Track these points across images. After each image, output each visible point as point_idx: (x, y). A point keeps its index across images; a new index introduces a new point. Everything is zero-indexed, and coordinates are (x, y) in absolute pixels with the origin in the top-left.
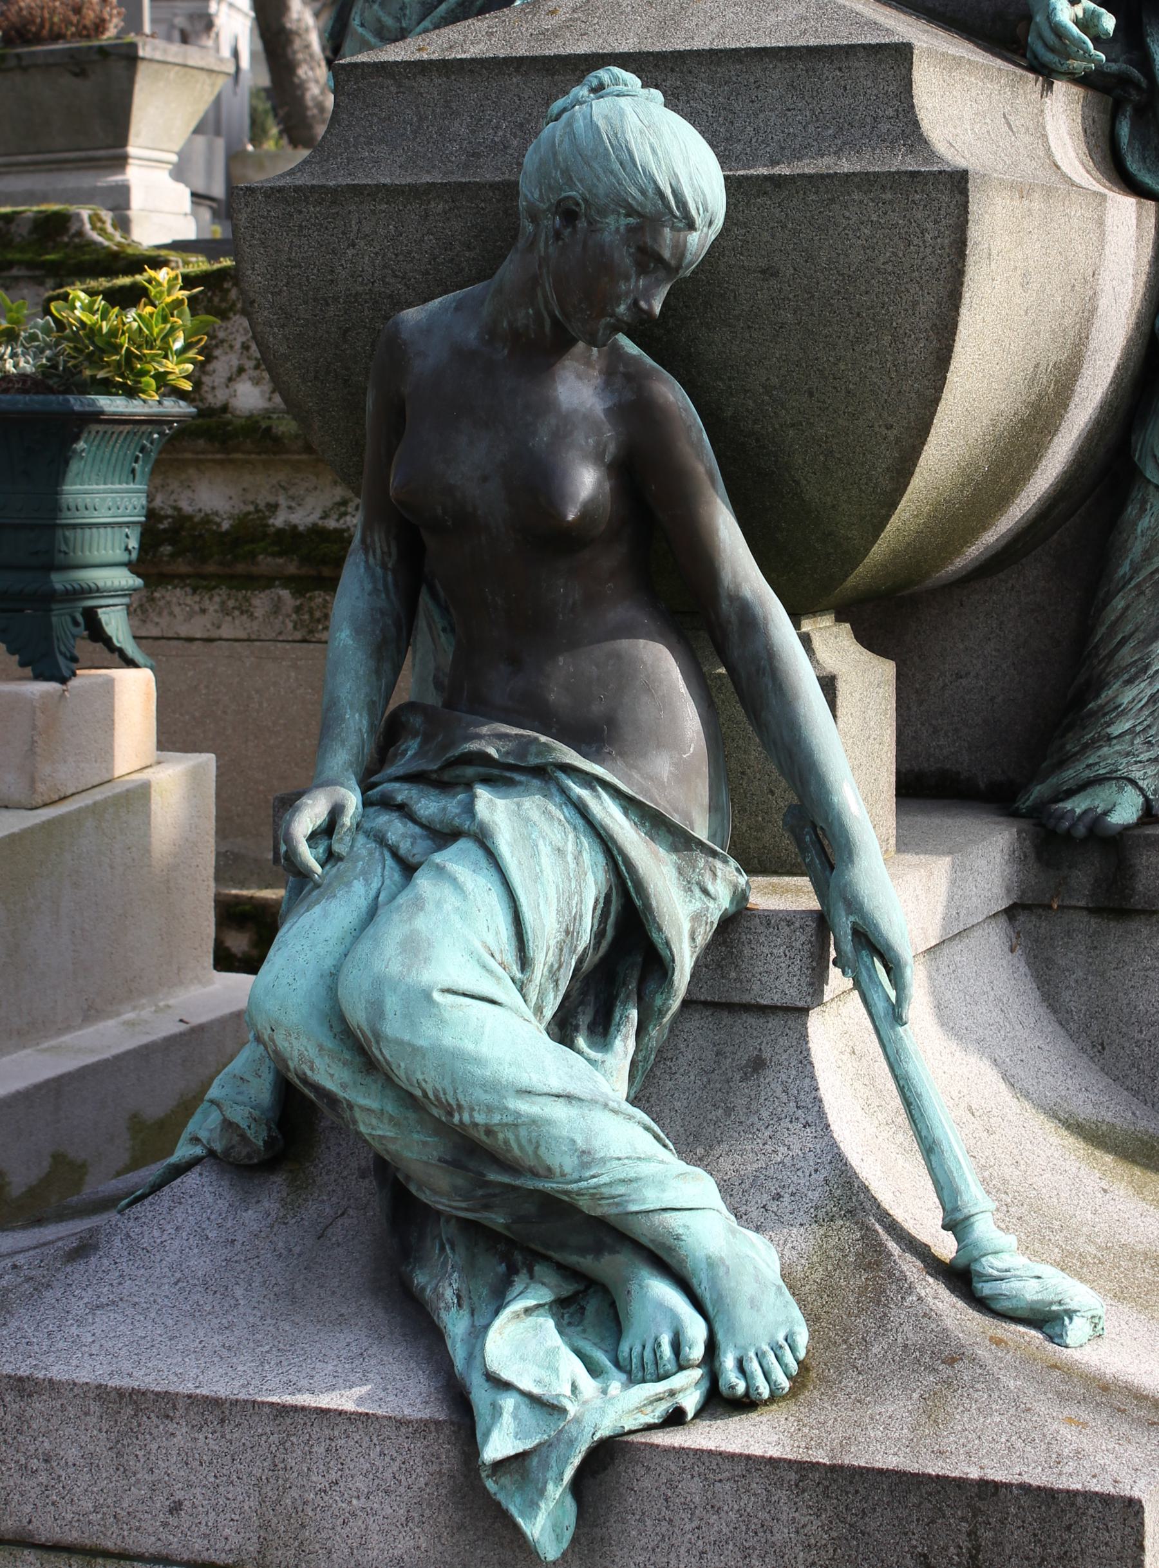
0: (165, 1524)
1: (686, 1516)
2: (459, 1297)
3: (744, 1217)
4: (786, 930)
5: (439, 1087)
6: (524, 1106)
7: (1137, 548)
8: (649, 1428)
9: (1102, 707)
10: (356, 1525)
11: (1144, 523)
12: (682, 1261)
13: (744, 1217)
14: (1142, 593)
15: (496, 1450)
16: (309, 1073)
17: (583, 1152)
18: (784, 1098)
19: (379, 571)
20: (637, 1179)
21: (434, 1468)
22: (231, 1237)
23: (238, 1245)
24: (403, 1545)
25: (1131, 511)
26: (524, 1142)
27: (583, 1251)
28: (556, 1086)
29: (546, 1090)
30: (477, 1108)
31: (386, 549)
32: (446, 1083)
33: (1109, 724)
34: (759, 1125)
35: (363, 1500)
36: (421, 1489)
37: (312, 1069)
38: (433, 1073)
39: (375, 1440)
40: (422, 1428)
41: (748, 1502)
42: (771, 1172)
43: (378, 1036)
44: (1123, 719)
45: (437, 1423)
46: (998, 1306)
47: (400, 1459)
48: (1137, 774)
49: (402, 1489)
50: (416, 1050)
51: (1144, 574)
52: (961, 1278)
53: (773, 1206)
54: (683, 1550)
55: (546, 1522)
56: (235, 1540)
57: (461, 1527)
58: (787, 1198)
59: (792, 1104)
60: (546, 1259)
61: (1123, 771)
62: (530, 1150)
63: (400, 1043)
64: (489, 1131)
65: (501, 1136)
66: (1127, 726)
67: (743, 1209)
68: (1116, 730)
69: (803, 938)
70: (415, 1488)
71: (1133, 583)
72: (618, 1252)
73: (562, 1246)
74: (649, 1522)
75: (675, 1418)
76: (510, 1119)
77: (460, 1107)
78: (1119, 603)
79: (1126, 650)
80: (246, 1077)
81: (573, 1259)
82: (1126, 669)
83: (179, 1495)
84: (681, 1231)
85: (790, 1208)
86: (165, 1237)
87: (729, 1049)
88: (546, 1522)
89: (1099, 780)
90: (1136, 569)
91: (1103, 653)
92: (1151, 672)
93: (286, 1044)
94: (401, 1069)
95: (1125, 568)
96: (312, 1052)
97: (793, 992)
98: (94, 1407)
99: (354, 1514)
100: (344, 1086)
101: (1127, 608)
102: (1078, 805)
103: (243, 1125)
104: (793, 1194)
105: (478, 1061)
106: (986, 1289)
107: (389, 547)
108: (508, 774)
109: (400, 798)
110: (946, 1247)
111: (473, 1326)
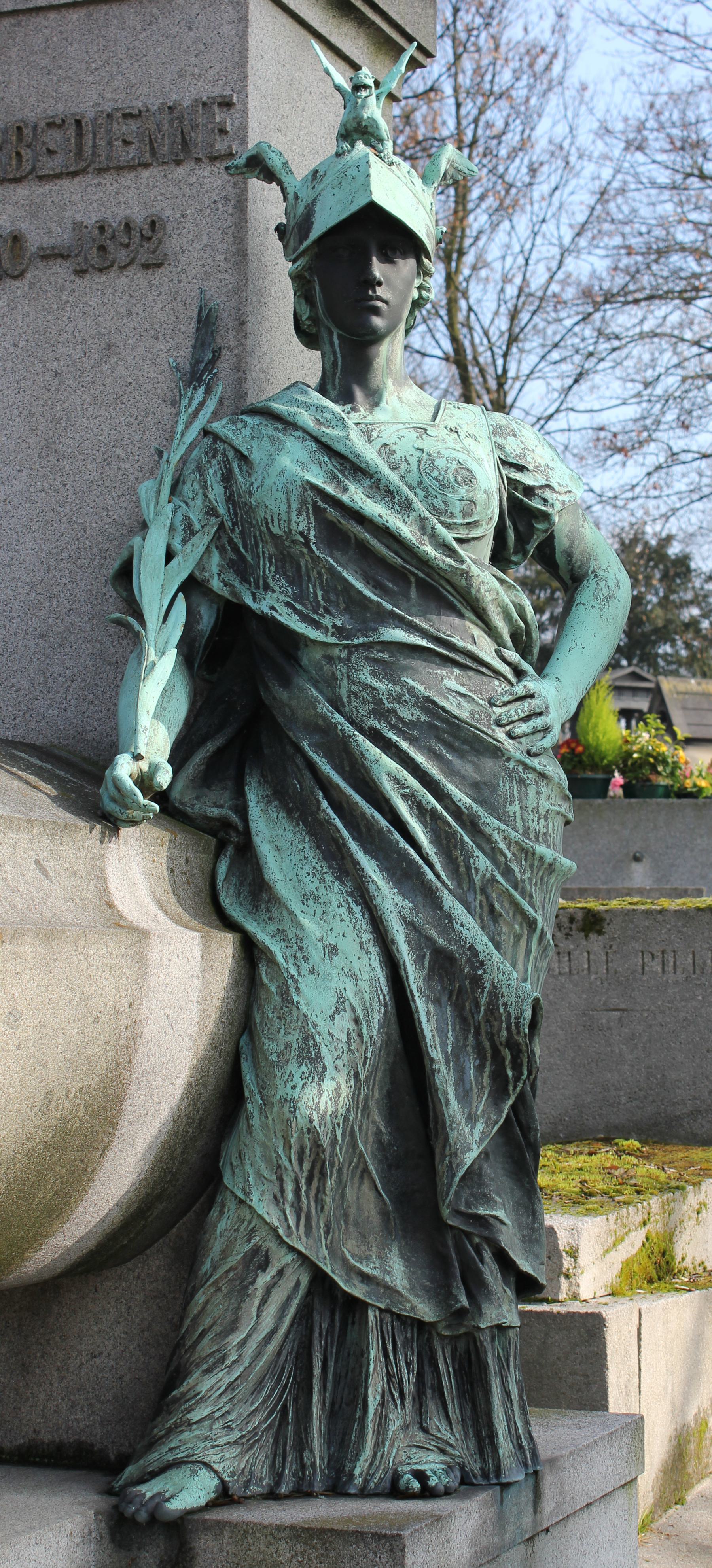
7: (217, 1247)
9: (183, 1394)
11: (222, 1225)
14: (219, 1289)
25: (214, 1213)
33: (189, 1410)
44: (203, 1406)
48: (212, 1457)
61: (199, 1455)
66: (206, 1412)
68: (195, 1416)
71: (212, 1280)
78: (200, 1298)
79: (205, 1341)
82: (204, 1359)
89: (176, 1464)
90: (215, 1268)
91: (189, 1343)
92: (228, 1362)
95: (207, 1267)
101: (207, 1302)
102: (149, 1490)
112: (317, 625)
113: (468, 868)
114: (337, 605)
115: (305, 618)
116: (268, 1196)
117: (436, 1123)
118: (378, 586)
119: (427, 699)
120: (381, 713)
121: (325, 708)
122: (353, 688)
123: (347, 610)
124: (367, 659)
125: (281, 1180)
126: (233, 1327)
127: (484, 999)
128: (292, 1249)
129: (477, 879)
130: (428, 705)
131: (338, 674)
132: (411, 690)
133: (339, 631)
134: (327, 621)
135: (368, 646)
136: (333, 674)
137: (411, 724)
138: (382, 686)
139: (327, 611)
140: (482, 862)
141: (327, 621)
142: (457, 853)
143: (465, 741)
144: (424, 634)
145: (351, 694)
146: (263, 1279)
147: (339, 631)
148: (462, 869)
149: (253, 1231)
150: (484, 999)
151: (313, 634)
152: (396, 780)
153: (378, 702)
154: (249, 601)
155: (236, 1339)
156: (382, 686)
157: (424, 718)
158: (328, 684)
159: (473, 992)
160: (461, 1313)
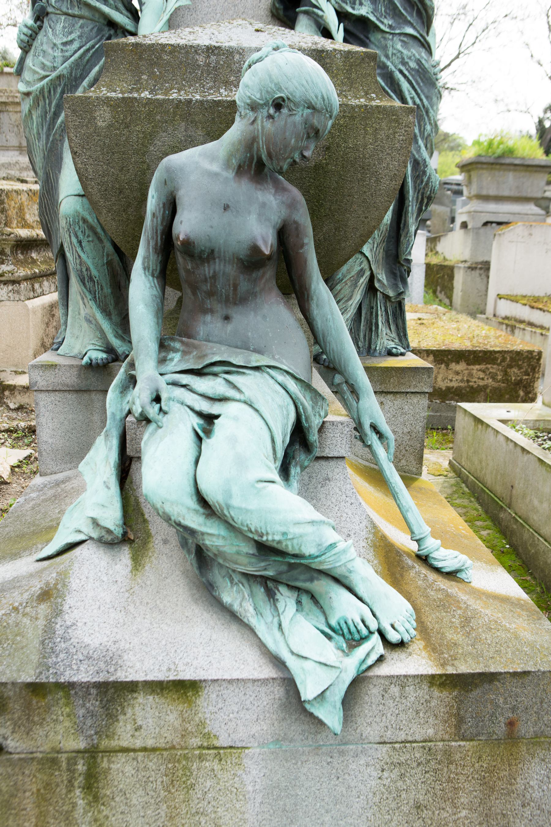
0: (133, 736)
1: (391, 701)
4: (340, 426)
5: (258, 526)
8: (370, 667)
10: (232, 725)
12: (351, 581)
16: (182, 521)
18: (340, 493)
19: (151, 278)
21: (272, 697)
22: (115, 580)
23: (119, 582)
24: (255, 729)
26: (295, 545)
27: (305, 581)
31: (155, 268)
34: (332, 505)
35: (235, 714)
36: (264, 707)
37: (184, 519)
39: (242, 689)
40: (265, 682)
41: (420, 693)
42: (342, 525)
43: (228, 507)
45: (273, 679)
46: (444, 570)
47: (254, 695)
49: (255, 708)
50: (247, 511)
51: (348, 277)
52: (424, 559)
54: (389, 715)
55: (331, 715)
56: (169, 738)
57: (284, 719)
58: (352, 535)
59: (344, 496)
60: (282, 583)
62: (297, 548)
63: (240, 509)
64: (279, 542)
65: (284, 544)
69: (348, 429)
70: (262, 706)
73: (296, 580)
74: (374, 706)
75: (381, 659)
77: (267, 534)
80: (106, 504)
81: (299, 584)
83: (139, 723)
84: (352, 569)
86: (83, 583)
87: (314, 475)
88: (331, 715)
90: (344, 276)
93: (171, 509)
94: (239, 518)
95: (340, 276)
96: (184, 511)
97: (343, 451)
98: (93, 691)
99: (230, 720)
100: (200, 525)
101: (341, 289)
103: (112, 528)
104: (355, 534)
107: (157, 266)
108: (241, 370)
109: (184, 382)
110: (414, 547)
111: (266, 623)
112: (382, 23)
113: (424, 129)
114: (389, 15)
115: (378, 19)
116: (369, 249)
117: (405, 225)
118: (405, 9)
119: (419, 60)
120: (404, 63)
121: (383, 59)
122: (394, 51)
123: (393, 18)
124: (400, 40)
125: (374, 243)
126: (350, 298)
127: (425, 179)
128: (371, 269)
129: (426, 134)
130: (419, 62)
131: (388, 45)
132: (414, 55)
133: (390, 26)
134: (386, 21)
135: (400, 34)
136: (386, 45)
137: (412, 69)
138: (405, 52)
139: (385, 17)
140: (428, 127)
141: (386, 21)
142: (422, 123)
143: (427, 79)
144: (418, 32)
145: (393, 54)
146: (362, 280)
147: (390, 26)
148: (422, 129)
149: (362, 262)
150: (425, 179)
151: (382, 27)
152: (409, 91)
153: (403, 59)
154: (350, 10)
155: (350, 303)
156: (405, 52)
157: (417, 67)
158: (385, 48)
159: (422, 176)
160: (402, 293)
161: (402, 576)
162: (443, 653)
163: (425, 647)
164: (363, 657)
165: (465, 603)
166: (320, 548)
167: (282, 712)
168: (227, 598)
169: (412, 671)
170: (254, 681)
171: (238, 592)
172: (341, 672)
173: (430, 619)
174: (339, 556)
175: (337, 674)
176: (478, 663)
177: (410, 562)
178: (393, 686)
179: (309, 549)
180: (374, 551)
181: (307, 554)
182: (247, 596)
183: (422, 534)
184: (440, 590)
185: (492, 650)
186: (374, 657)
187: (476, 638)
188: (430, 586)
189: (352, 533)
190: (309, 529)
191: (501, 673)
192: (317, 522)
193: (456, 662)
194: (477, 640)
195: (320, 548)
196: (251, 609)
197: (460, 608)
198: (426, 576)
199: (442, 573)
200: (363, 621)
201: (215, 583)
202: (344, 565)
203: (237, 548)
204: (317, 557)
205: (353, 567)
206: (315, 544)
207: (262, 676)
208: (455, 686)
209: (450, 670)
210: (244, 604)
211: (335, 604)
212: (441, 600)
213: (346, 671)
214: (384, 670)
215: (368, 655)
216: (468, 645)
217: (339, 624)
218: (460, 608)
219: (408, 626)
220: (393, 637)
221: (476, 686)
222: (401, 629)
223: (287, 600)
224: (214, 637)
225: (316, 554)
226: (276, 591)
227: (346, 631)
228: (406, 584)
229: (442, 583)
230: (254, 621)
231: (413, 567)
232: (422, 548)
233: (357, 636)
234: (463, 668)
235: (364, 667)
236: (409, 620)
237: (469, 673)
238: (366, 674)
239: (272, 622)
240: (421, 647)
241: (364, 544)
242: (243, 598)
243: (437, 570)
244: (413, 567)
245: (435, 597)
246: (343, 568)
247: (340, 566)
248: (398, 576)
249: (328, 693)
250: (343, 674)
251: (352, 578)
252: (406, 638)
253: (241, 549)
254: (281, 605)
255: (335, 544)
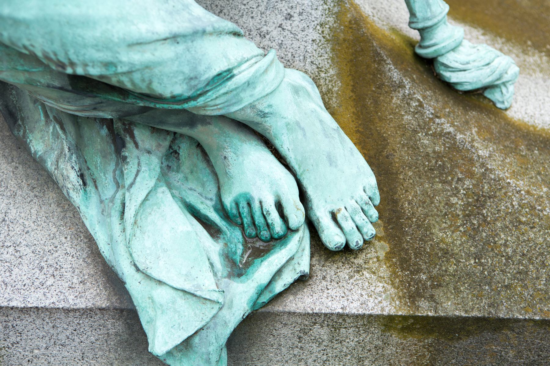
2: (82, 176)
3: (267, 37)
5: (47, 50)
6: (136, 57)
13: (267, 37)
15: (166, 343)
17: (191, 79)
20: (236, 89)
27: (179, 125)
28: (162, 29)
29: (155, 37)
30: (91, 64)
32: (57, 46)
35: (43, 350)
38: (40, 40)
45: (102, 309)
46: (460, 88)
47: (71, 329)
52: (428, 66)
53: (287, 25)
58: (296, 17)
67: (264, 29)
72: (209, 124)
75: (302, 280)
76: (125, 69)
77: (72, 64)
84: (267, 111)
85: (301, 27)
104: (300, 14)
105: (87, 22)
106: (453, 78)
111: (102, 202)
161: (376, 102)
162: (419, 271)
163: (389, 256)
164: (265, 280)
165: (483, 165)
166: (193, 83)
167: (124, 351)
168: (37, 146)
169: (354, 308)
170: (67, 311)
171: (56, 136)
172: (220, 309)
173: (410, 198)
174: (238, 94)
175: (214, 312)
176: (479, 297)
177: (396, 75)
178: (317, 326)
179: (171, 86)
180: (333, 50)
181: (167, 94)
182: (67, 150)
183: (428, 19)
184: (442, 134)
185: (512, 269)
186: (288, 278)
187: (488, 243)
188: (425, 127)
189: (295, 13)
190: (166, 52)
191: (517, 320)
192: (184, 36)
193: (438, 293)
194: (489, 245)
195: (193, 83)
196: (73, 176)
197: (471, 175)
198: (421, 105)
199: (457, 91)
200: (279, 207)
201: (20, 110)
202: (252, 106)
203: (27, 75)
204: (189, 99)
205: (270, 106)
206: (181, 77)
207: (82, 304)
208: (430, 332)
209: (425, 309)
210: (62, 166)
211: (233, 170)
212: (439, 156)
213: (230, 307)
214: (304, 302)
215: (279, 272)
216: (468, 256)
217: (237, 204)
218: (471, 175)
219: (361, 219)
220: (332, 237)
221: (469, 334)
222: (348, 225)
223: (144, 158)
224: (13, 213)
225: (187, 94)
226: (128, 139)
227: (247, 220)
228: (381, 119)
229: (450, 122)
230: (77, 198)
231: (401, 86)
232: (427, 43)
233: (265, 234)
234: (450, 307)
235: (265, 298)
236: (366, 208)
237: (458, 317)
238: (270, 308)
239: (114, 197)
240: (382, 254)
241: (316, 36)
242: (61, 154)
243: (449, 88)
244: (401, 86)
245: (429, 150)
246: (249, 111)
247: (242, 109)
248: (369, 102)
249: (197, 340)
250: (224, 312)
251: (267, 125)
252: (356, 240)
253: (34, 77)
254: (130, 170)
255: (229, 71)
